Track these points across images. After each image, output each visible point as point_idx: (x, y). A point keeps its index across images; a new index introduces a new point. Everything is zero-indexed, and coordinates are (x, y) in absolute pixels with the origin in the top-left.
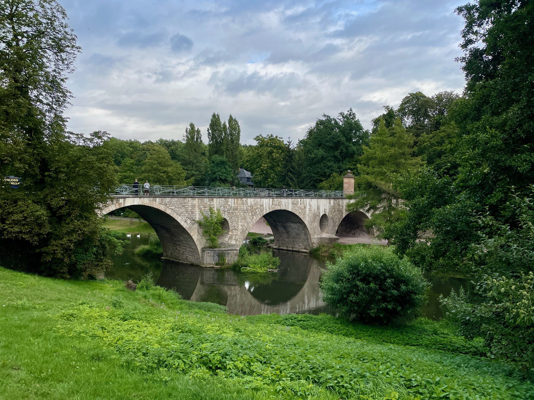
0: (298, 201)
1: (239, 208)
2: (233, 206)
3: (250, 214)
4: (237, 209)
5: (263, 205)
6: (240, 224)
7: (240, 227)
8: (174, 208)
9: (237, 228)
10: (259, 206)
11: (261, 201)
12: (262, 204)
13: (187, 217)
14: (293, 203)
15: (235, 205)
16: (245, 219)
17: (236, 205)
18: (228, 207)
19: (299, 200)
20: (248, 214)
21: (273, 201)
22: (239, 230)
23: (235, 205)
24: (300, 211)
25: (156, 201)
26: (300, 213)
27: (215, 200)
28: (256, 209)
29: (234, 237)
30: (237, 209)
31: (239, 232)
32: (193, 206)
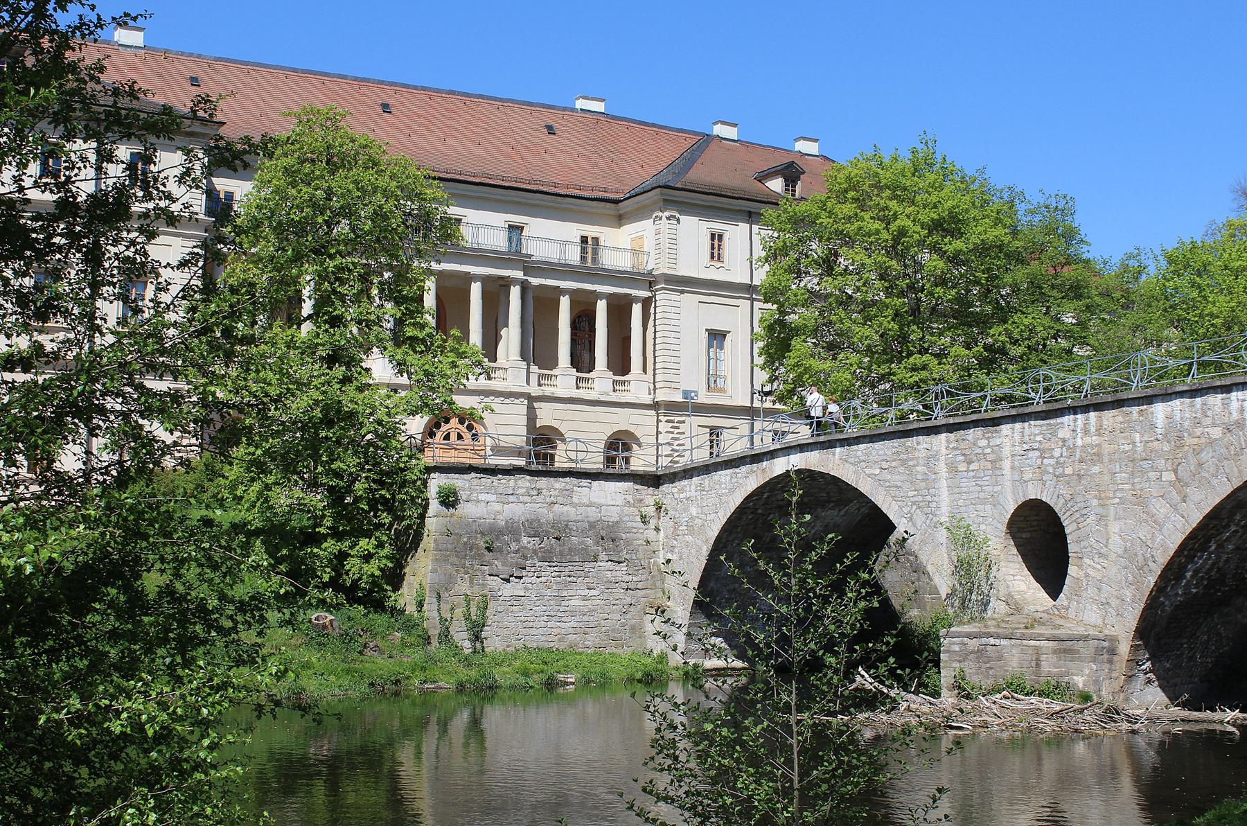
1: (1107, 448)
2: (1079, 442)
3: (1169, 476)
4: (1098, 454)
7: (1116, 544)
8: (877, 471)
9: (1104, 550)
10: (1216, 432)
11: (1226, 405)
12: (1235, 416)
13: (914, 503)
15: (1088, 440)
16: (1141, 500)
17: (1095, 439)
18: (1057, 453)
20: (1153, 475)
22: (1113, 557)
23: (1088, 440)
25: (834, 455)
30: (1098, 454)
32: (933, 457)
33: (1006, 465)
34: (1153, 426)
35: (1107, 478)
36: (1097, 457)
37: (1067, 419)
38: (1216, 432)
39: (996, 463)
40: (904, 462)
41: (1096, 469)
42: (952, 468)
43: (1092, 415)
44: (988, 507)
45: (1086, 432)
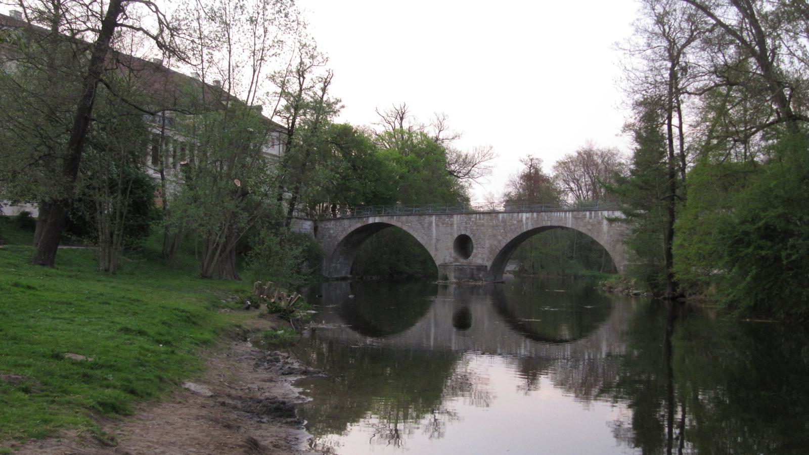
0: (586, 215)
5: (522, 221)
6: (487, 242)
7: (487, 245)
10: (515, 222)
11: (518, 216)
14: (574, 217)
19: (588, 213)
21: (538, 215)
24: (590, 227)
26: (589, 230)
27: (455, 216)
28: (511, 225)
29: (480, 256)
31: (487, 251)
32: (430, 223)
33: (455, 226)
34: (499, 220)
35: (485, 231)
36: (483, 225)
37: (474, 215)
38: (515, 222)
39: (452, 225)
40: (420, 223)
41: (483, 228)
42: (437, 225)
43: (459, 216)
44: (449, 236)
45: (480, 219)
